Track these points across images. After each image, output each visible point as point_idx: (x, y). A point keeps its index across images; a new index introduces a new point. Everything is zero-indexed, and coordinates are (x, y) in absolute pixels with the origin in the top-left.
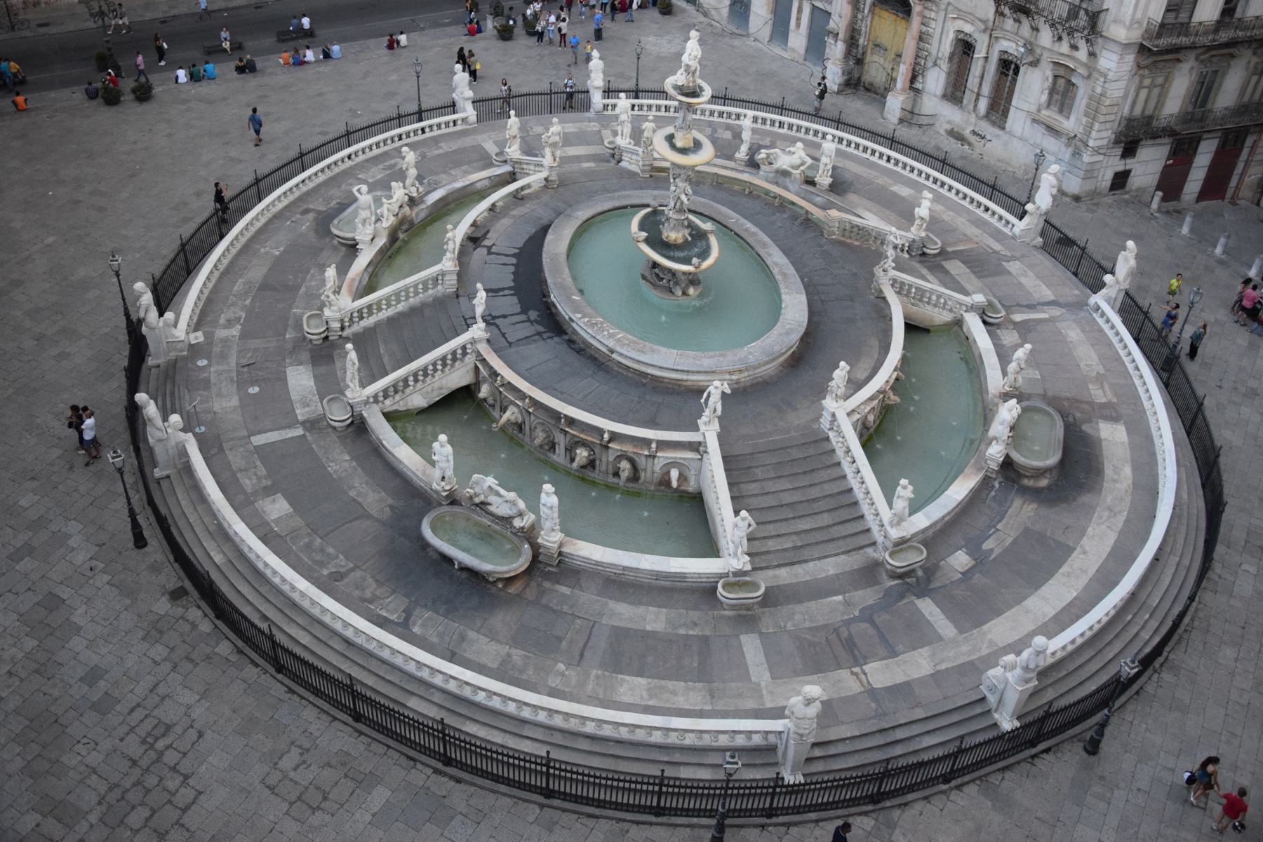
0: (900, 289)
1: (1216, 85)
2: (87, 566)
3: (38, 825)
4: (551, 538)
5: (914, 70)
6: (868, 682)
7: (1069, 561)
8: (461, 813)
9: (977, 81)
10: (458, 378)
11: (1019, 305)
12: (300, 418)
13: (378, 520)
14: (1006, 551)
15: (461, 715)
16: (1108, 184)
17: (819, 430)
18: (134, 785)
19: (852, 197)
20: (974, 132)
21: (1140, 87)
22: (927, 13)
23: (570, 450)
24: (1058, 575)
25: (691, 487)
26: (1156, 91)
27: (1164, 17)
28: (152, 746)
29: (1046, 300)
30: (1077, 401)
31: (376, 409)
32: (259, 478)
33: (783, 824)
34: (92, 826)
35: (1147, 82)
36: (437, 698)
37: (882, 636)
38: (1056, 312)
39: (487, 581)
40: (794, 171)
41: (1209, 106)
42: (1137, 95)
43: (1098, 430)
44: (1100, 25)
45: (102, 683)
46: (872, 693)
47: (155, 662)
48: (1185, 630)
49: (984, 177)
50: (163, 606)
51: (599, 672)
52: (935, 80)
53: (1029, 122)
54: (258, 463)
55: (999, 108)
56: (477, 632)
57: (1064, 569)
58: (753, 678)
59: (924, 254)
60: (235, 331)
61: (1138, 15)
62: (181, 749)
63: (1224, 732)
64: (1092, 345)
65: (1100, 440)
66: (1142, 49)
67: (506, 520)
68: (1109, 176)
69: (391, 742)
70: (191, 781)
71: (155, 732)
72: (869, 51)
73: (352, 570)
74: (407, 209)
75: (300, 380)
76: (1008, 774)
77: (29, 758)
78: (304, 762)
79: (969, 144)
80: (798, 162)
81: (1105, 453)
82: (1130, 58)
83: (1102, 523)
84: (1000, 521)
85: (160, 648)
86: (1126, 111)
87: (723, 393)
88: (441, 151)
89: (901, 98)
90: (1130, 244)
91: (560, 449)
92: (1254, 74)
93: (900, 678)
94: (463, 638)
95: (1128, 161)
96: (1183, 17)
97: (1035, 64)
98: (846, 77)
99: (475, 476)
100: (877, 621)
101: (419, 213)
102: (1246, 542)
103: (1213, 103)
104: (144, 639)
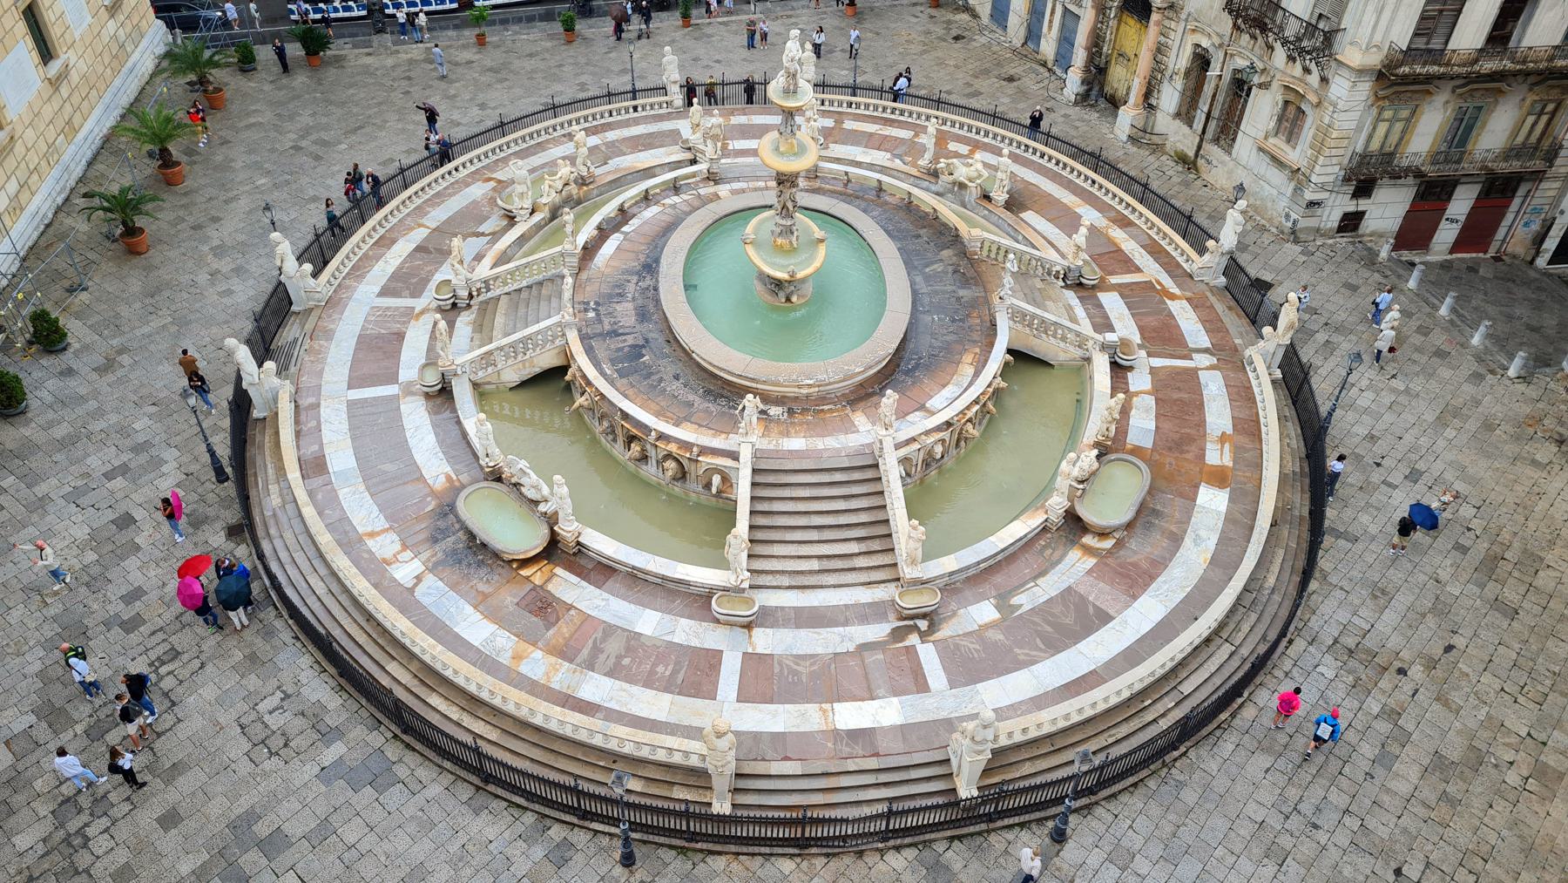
0: (1017, 316)
1: (1479, 124)
5: (1149, 83)
10: (547, 359)
16: (1336, 225)
21: (1378, 119)
22: (1166, 23)
26: (1399, 126)
36: (414, 667)
41: (1469, 147)
42: (1374, 129)
44: (1336, 47)
45: (138, 603)
48: (1219, 727)
52: (1169, 98)
53: (1255, 150)
55: (1227, 128)
59: (1081, 284)
61: (1378, 38)
62: (180, 678)
66: (1380, 76)
71: (164, 658)
77: (48, 663)
78: (282, 707)
80: (975, 174)
82: (1365, 87)
86: (1359, 148)
89: (1133, 113)
92: (1529, 114)
93: (866, 724)
95: (1361, 202)
96: (1436, 44)
102: (1336, 641)
103: (1475, 144)
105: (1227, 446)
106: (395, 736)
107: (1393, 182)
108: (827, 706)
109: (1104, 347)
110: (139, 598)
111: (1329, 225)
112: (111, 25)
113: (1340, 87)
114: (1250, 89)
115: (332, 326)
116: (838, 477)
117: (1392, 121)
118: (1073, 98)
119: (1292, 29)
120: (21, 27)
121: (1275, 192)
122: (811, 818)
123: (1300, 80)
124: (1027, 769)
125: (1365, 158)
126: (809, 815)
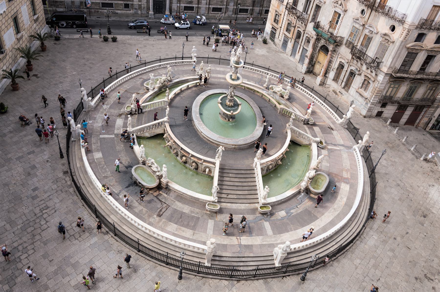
0: (293, 131)
1: (415, 91)
2: (46, 160)
3: (5, 225)
5: (326, 71)
8: (114, 250)
9: (343, 77)
10: (159, 131)
11: (331, 144)
12: (115, 133)
14: (298, 214)
16: (375, 114)
17: (252, 167)
18: (33, 221)
20: (340, 92)
21: (390, 87)
26: (395, 89)
28: (42, 211)
29: (340, 144)
30: (338, 175)
32: (97, 146)
33: (201, 277)
34: (18, 229)
38: (342, 148)
40: (278, 93)
41: (412, 97)
43: (341, 185)
44: (380, 67)
45: (37, 192)
46: (240, 245)
47: (52, 189)
48: (346, 251)
49: (336, 105)
50: (61, 175)
52: (332, 75)
53: (355, 91)
54: (99, 142)
55: (347, 86)
59: (308, 124)
61: (392, 65)
62: (49, 214)
63: (347, 285)
65: (340, 188)
70: (48, 223)
71: (44, 208)
72: (316, 63)
75: (119, 122)
76: (274, 279)
77: (10, 207)
79: (338, 95)
84: (299, 205)
85: (55, 186)
86: (384, 94)
87: (223, 150)
89: (321, 78)
90: (368, 132)
92: (429, 90)
95: (383, 109)
97: (360, 75)
102: (377, 229)
103: (414, 96)
105: (349, 173)
107: (391, 104)
108: (238, 238)
109: (315, 142)
110: (37, 190)
111: (374, 114)
112: (35, 25)
113: (381, 77)
114: (355, 75)
115: (95, 116)
116: (243, 172)
117: (393, 88)
118: (304, 72)
119: (368, 61)
120: (12, 24)
121: (360, 104)
122: (235, 269)
123: (369, 74)
124: (295, 259)
125: (385, 97)
126: (234, 268)
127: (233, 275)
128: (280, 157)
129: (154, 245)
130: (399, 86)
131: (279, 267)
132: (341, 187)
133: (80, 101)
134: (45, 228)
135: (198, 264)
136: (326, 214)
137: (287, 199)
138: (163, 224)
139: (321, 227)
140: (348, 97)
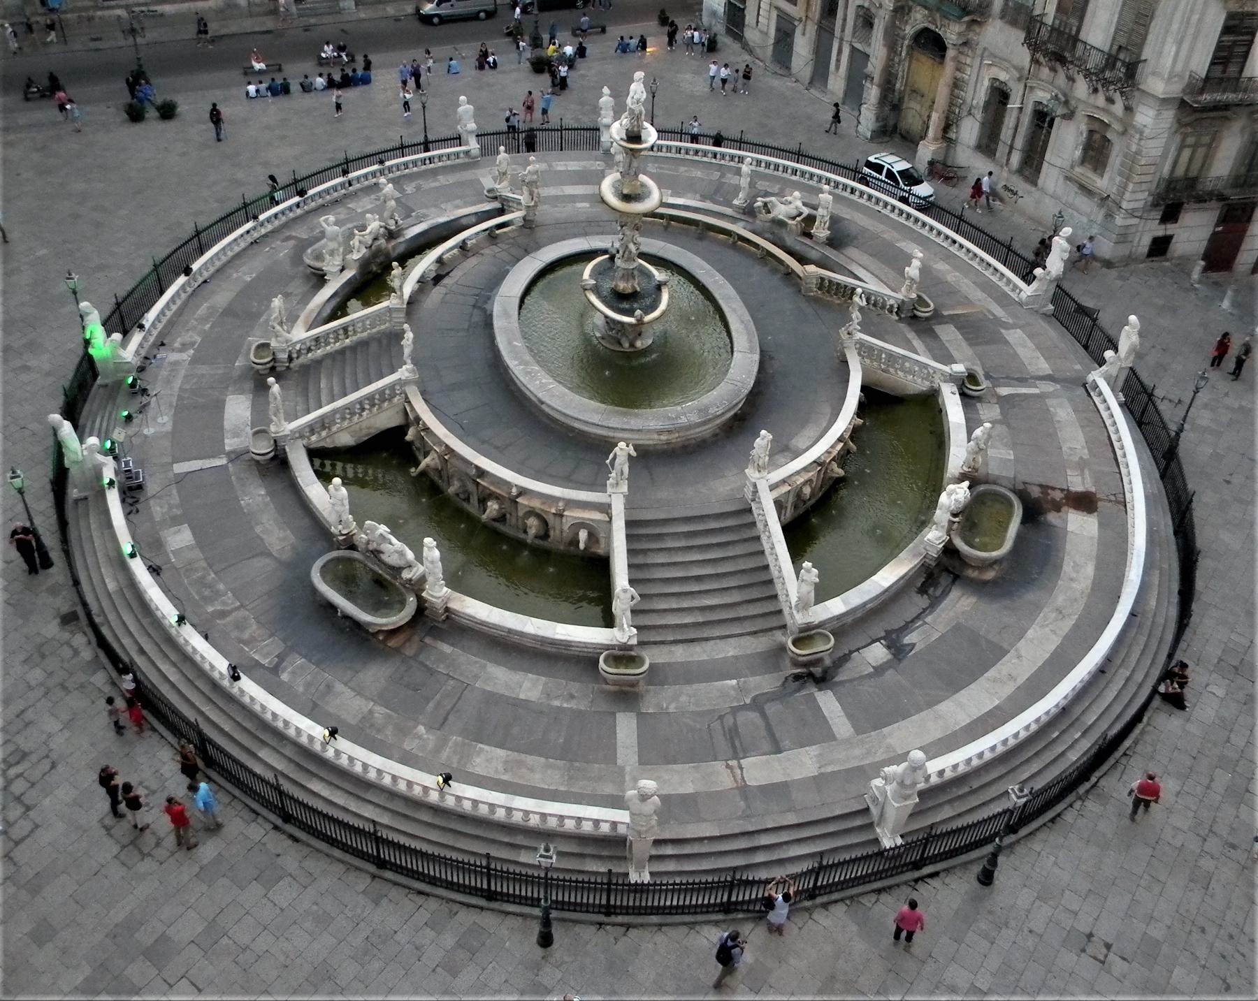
0: (866, 351)
4: (438, 593)
5: (947, 118)
6: (743, 778)
7: (998, 665)
8: (290, 875)
9: (1010, 132)
10: (386, 419)
11: (1007, 377)
12: (227, 448)
13: (275, 558)
14: (931, 648)
15: (308, 771)
16: (1146, 250)
17: (743, 499)
19: (852, 252)
22: (962, 58)
23: (483, 501)
24: (982, 680)
25: (601, 551)
26: (1201, 152)
27: (1209, 71)
31: (300, 443)
32: (171, 507)
33: (622, 925)
35: (1190, 140)
36: (288, 751)
37: (769, 729)
38: (1049, 387)
39: (367, 632)
40: (790, 222)
42: (1178, 156)
43: (1066, 521)
46: (743, 790)
47: (29, 687)
49: (1000, 236)
50: (52, 629)
51: (460, 739)
52: (969, 131)
53: (1061, 179)
56: (346, 684)
57: (991, 673)
58: (619, 762)
59: (915, 317)
60: (186, 356)
61: (1179, 67)
62: (32, 779)
64: (1081, 426)
65: (1066, 532)
66: (1183, 104)
67: (397, 570)
68: (1146, 241)
69: (237, 792)
70: (31, 813)
72: (906, 99)
73: (237, 609)
74: (382, 241)
75: (238, 409)
79: (1002, 200)
80: (794, 212)
81: (1068, 547)
82: (1169, 114)
83: (1047, 625)
87: (629, 455)
88: (437, 184)
89: (932, 148)
90: (1133, 318)
91: (474, 500)
93: (779, 778)
94: (329, 687)
95: (1169, 226)
97: (1069, 116)
98: (881, 124)
99: (368, 522)
100: (768, 712)
101: (397, 246)
104: (24, 662)
105: (1087, 472)
106: (276, 828)
107: (1198, 206)
108: (733, 763)
109: (952, 378)
113: (1145, 116)
114: (1052, 120)
117: (1195, 147)
118: (869, 135)
119: (1094, 61)
122: (740, 880)
123: (1103, 110)
124: (947, 812)
125: (1171, 184)
126: (738, 877)
127: (737, 903)
128: (835, 452)
129: (434, 836)
130: (1213, 139)
131: (896, 847)
132: (1071, 527)
133: (80, 352)
134: (25, 833)
135: (605, 881)
136: (1030, 633)
137: (883, 598)
138: (455, 752)
139: (1021, 680)
140: (1038, 202)
